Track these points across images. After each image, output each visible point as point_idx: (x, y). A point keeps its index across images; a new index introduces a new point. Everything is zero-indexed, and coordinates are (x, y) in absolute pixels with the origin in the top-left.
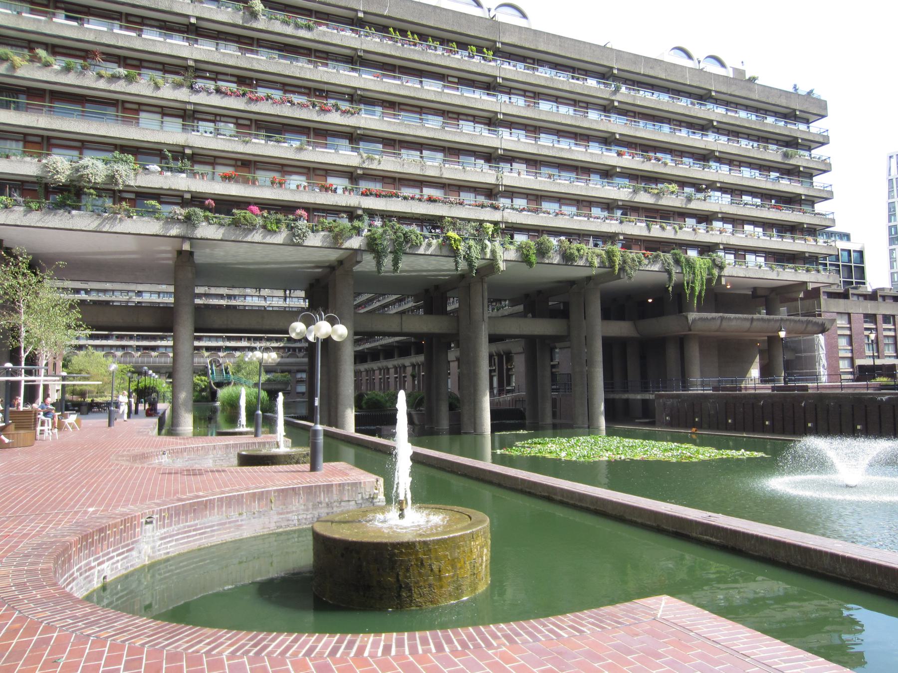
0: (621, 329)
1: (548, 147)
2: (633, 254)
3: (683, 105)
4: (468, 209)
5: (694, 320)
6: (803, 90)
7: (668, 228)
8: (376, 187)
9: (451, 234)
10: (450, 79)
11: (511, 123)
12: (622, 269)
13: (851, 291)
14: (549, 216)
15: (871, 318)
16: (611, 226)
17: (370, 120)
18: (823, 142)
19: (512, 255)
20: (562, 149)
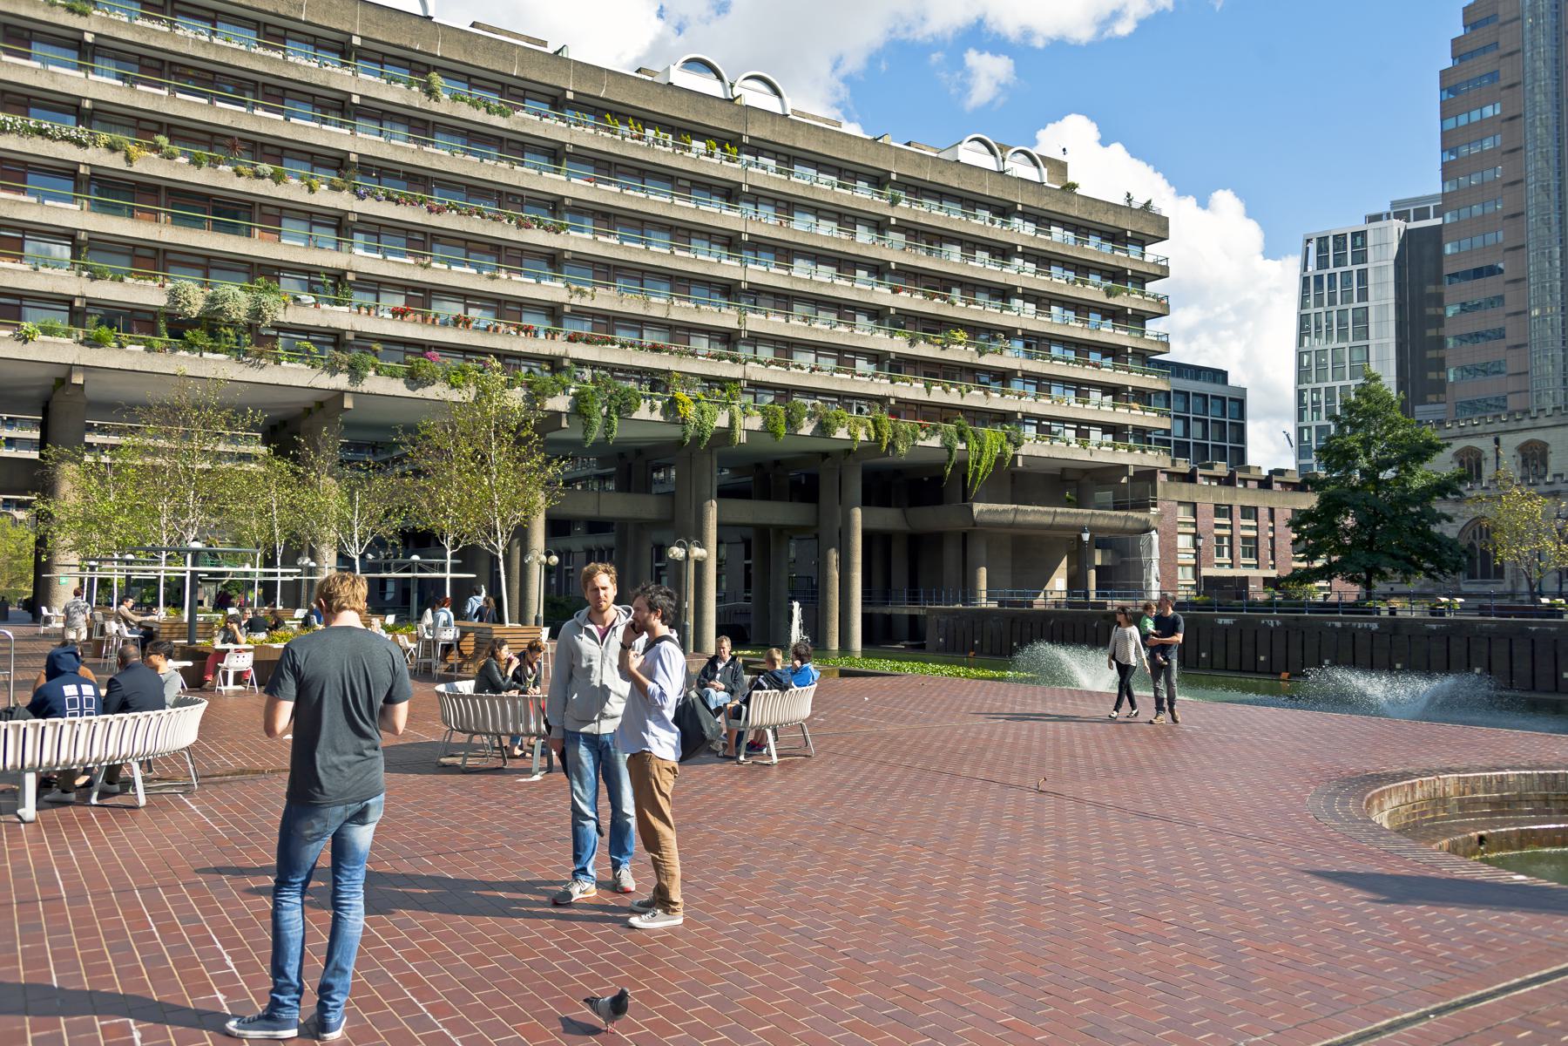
0: (889, 518)
1: (804, 281)
2: (905, 424)
3: (981, 224)
4: (703, 362)
5: (981, 512)
6: (1138, 202)
7: (953, 390)
8: (585, 328)
9: (681, 395)
10: (681, 182)
11: (758, 246)
12: (892, 445)
13: (1199, 471)
14: (802, 372)
15: (1220, 511)
16: (881, 387)
17: (579, 240)
18: (1162, 273)
19: (755, 423)
20: (822, 284)
